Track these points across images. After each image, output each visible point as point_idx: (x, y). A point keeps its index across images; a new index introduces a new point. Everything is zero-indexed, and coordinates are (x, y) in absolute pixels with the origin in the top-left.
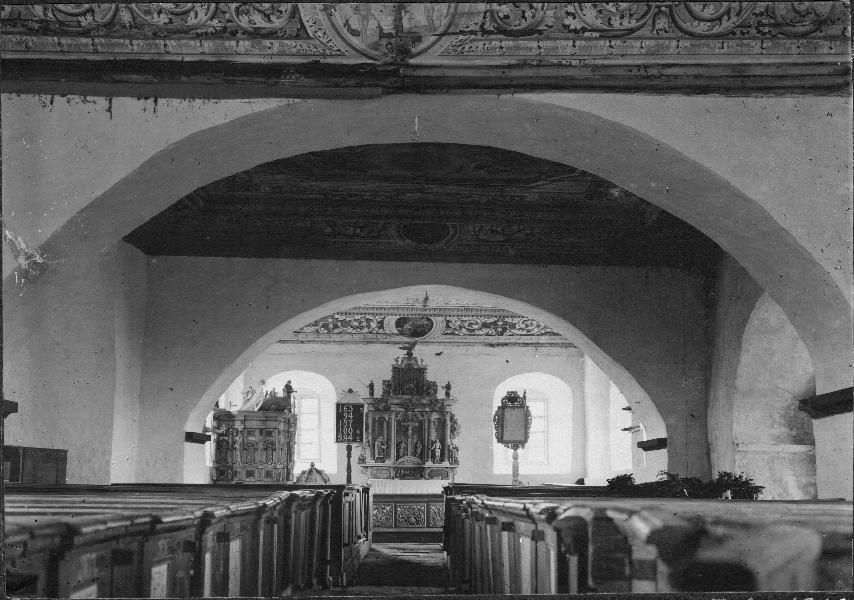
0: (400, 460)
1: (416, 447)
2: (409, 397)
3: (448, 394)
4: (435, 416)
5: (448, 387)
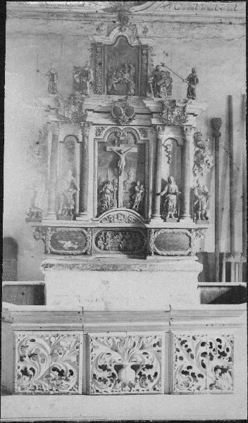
0: (104, 215)
1: (133, 192)
2: (123, 97)
3: (191, 93)
4: (167, 135)
5: (192, 80)
